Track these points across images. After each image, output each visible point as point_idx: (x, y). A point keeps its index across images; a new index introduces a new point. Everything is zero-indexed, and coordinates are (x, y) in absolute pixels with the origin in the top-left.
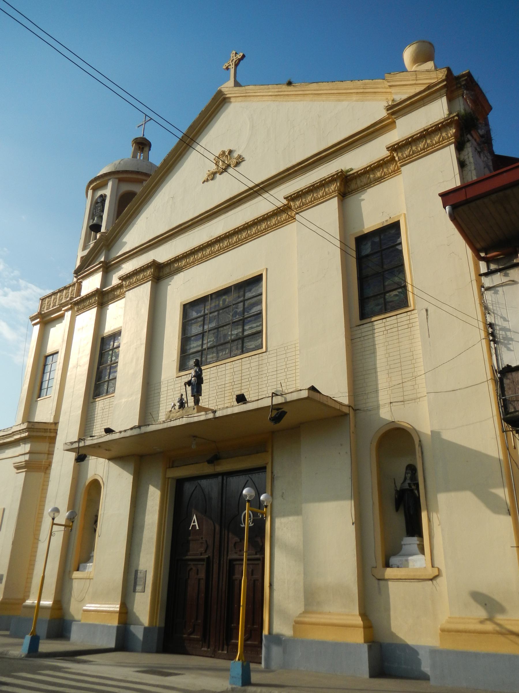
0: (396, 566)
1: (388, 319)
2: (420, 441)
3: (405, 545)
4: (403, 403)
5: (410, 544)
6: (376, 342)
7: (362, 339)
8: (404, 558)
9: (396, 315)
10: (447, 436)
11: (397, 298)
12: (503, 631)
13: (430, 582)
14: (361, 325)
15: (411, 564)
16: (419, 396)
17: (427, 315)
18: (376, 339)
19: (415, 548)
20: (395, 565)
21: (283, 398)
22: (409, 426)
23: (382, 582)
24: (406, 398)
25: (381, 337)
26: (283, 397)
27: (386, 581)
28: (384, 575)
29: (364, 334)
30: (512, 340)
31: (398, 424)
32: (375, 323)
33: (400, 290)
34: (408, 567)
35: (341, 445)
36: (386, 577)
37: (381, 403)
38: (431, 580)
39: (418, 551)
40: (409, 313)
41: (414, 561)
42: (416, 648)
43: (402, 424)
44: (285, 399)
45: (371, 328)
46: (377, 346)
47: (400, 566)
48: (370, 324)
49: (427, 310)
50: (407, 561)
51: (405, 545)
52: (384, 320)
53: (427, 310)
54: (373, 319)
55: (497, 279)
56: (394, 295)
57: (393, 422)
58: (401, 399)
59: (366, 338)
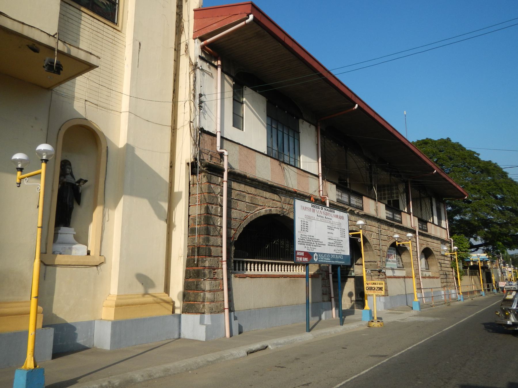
0: (58, 253)
1: (95, 20)
2: (107, 147)
3: (61, 234)
4: (96, 106)
5: (66, 234)
6: (81, 34)
7: (66, 19)
8: (67, 246)
9: (105, 23)
10: (138, 153)
11: (104, 7)
12: (159, 301)
13: (95, 268)
14: (67, 3)
15: (74, 252)
16: (111, 108)
17: (140, 48)
18: (81, 30)
19: (71, 238)
20: (57, 252)
21: (66, 48)
22: (100, 130)
23: (49, 268)
24: (99, 103)
25: (86, 32)
26: (65, 45)
27: (54, 266)
28: (54, 261)
29: (68, 15)
30: (206, 112)
31: (92, 124)
32: (83, 14)
33: (108, 3)
34: (70, 254)
35: (36, 119)
36: (56, 263)
37: (76, 95)
38: (97, 266)
39: (75, 241)
40: (115, 31)
41: (77, 249)
42: (73, 325)
43: (94, 125)
44: (69, 50)
45: (77, 15)
46: (81, 38)
47: (62, 253)
48: (78, 11)
49: (140, 44)
50: (70, 249)
51: (61, 234)
52: (91, 18)
53: (140, 44)
54: (82, 9)
55: (205, 66)
56: (102, 2)
57: (85, 119)
58: (96, 102)
59: (70, 21)
